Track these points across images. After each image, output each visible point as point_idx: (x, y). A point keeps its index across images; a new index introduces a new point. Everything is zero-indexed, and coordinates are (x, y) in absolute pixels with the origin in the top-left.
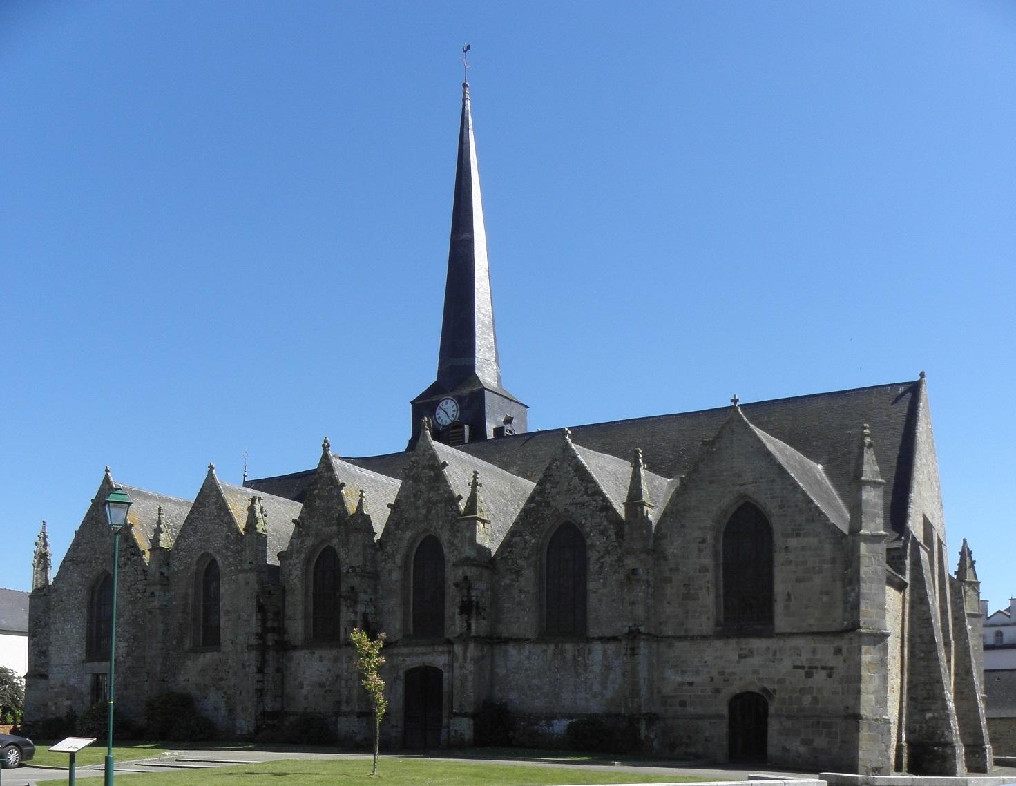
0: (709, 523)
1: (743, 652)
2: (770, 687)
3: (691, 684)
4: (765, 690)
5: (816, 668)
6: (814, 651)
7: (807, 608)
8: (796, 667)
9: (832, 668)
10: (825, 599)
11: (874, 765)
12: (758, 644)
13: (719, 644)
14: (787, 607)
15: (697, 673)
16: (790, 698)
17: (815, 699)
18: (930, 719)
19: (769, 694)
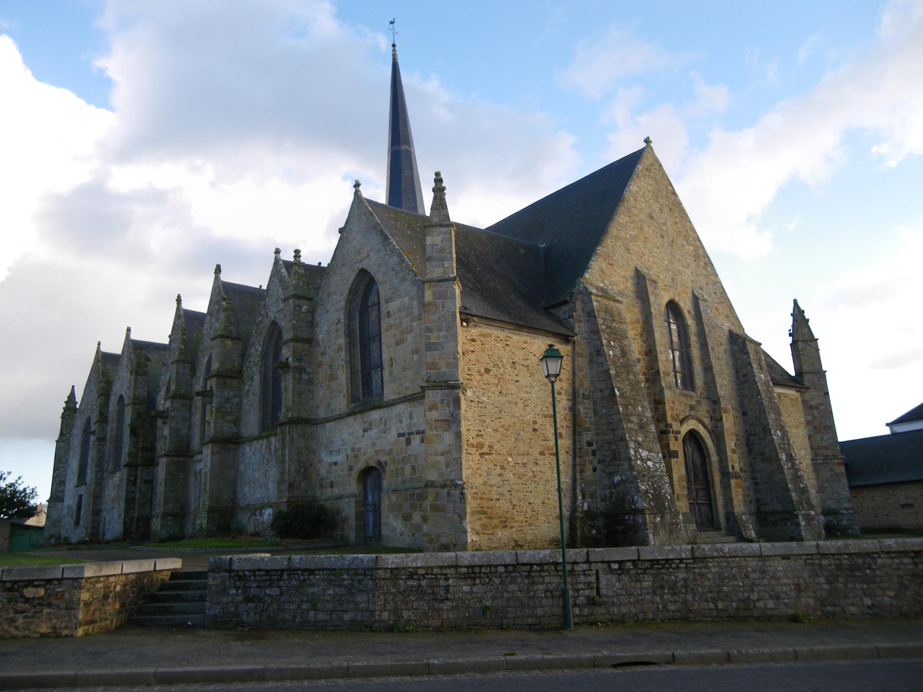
0: (343, 303)
1: (366, 425)
2: (383, 459)
3: (336, 463)
4: (379, 463)
5: (412, 433)
6: (411, 417)
7: (404, 370)
8: (400, 435)
9: (424, 432)
10: (416, 357)
11: (444, 540)
12: (375, 415)
13: (350, 420)
14: (391, 373)
15: (339, 452)
16: (397, 468)
17: (413, 468)
18: (618, 483)
19: (382, 465)
